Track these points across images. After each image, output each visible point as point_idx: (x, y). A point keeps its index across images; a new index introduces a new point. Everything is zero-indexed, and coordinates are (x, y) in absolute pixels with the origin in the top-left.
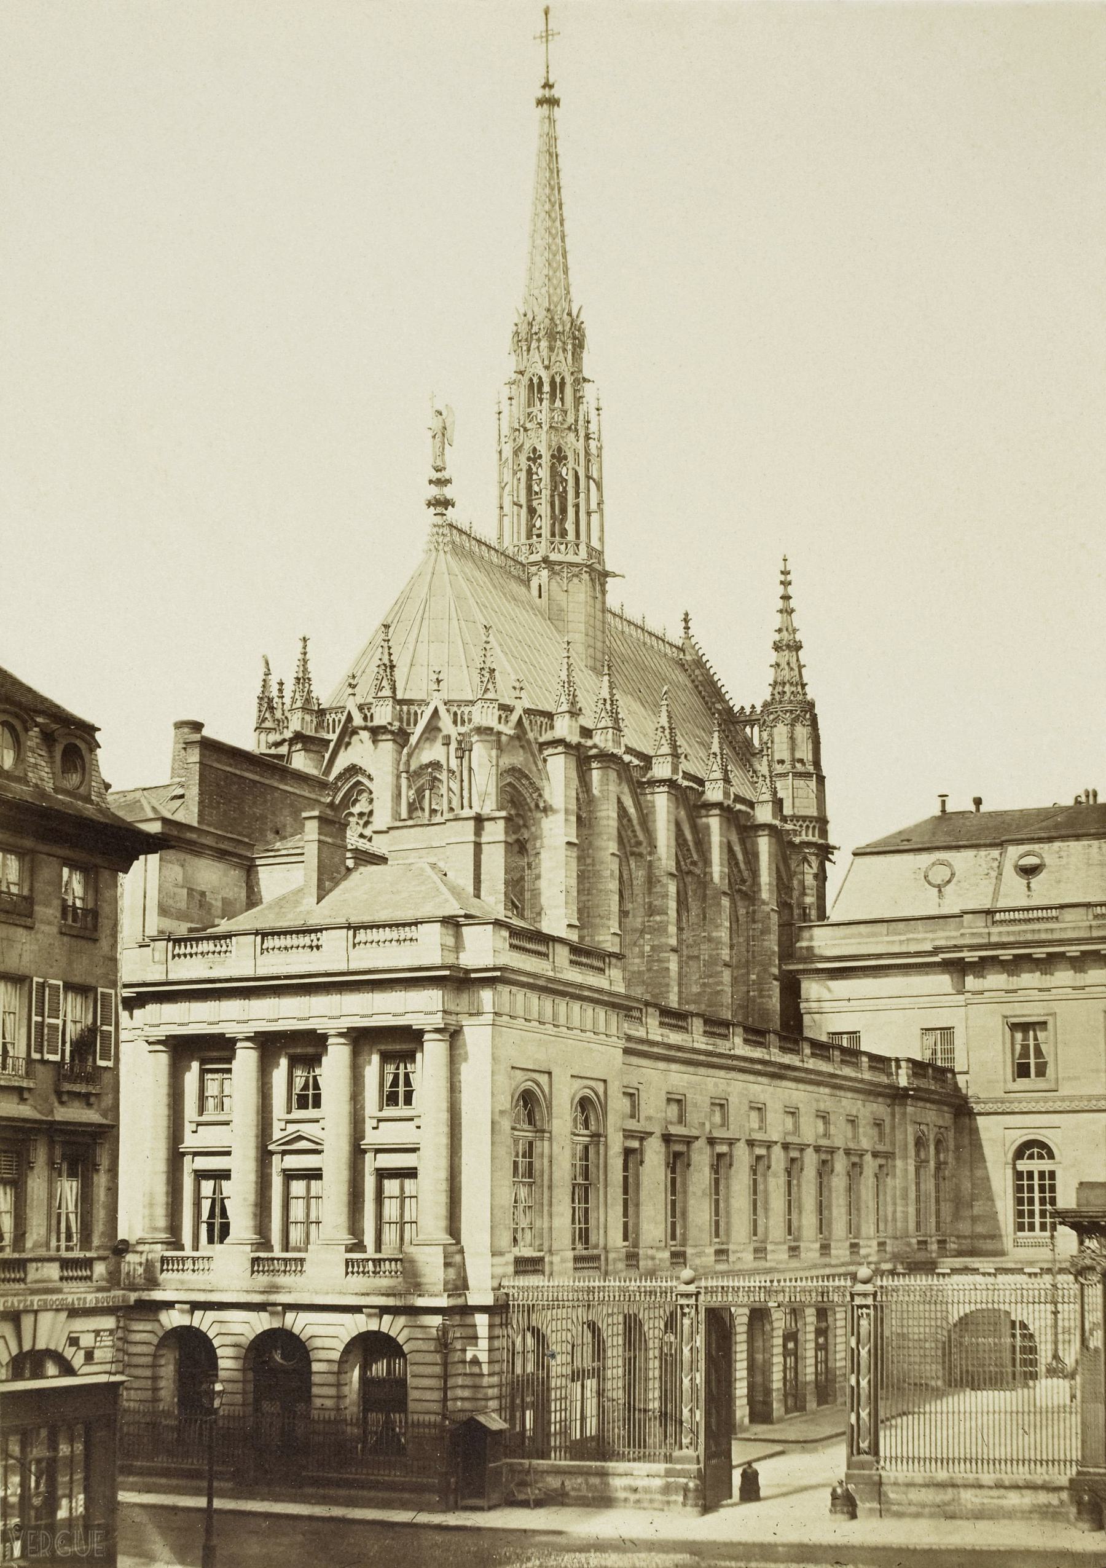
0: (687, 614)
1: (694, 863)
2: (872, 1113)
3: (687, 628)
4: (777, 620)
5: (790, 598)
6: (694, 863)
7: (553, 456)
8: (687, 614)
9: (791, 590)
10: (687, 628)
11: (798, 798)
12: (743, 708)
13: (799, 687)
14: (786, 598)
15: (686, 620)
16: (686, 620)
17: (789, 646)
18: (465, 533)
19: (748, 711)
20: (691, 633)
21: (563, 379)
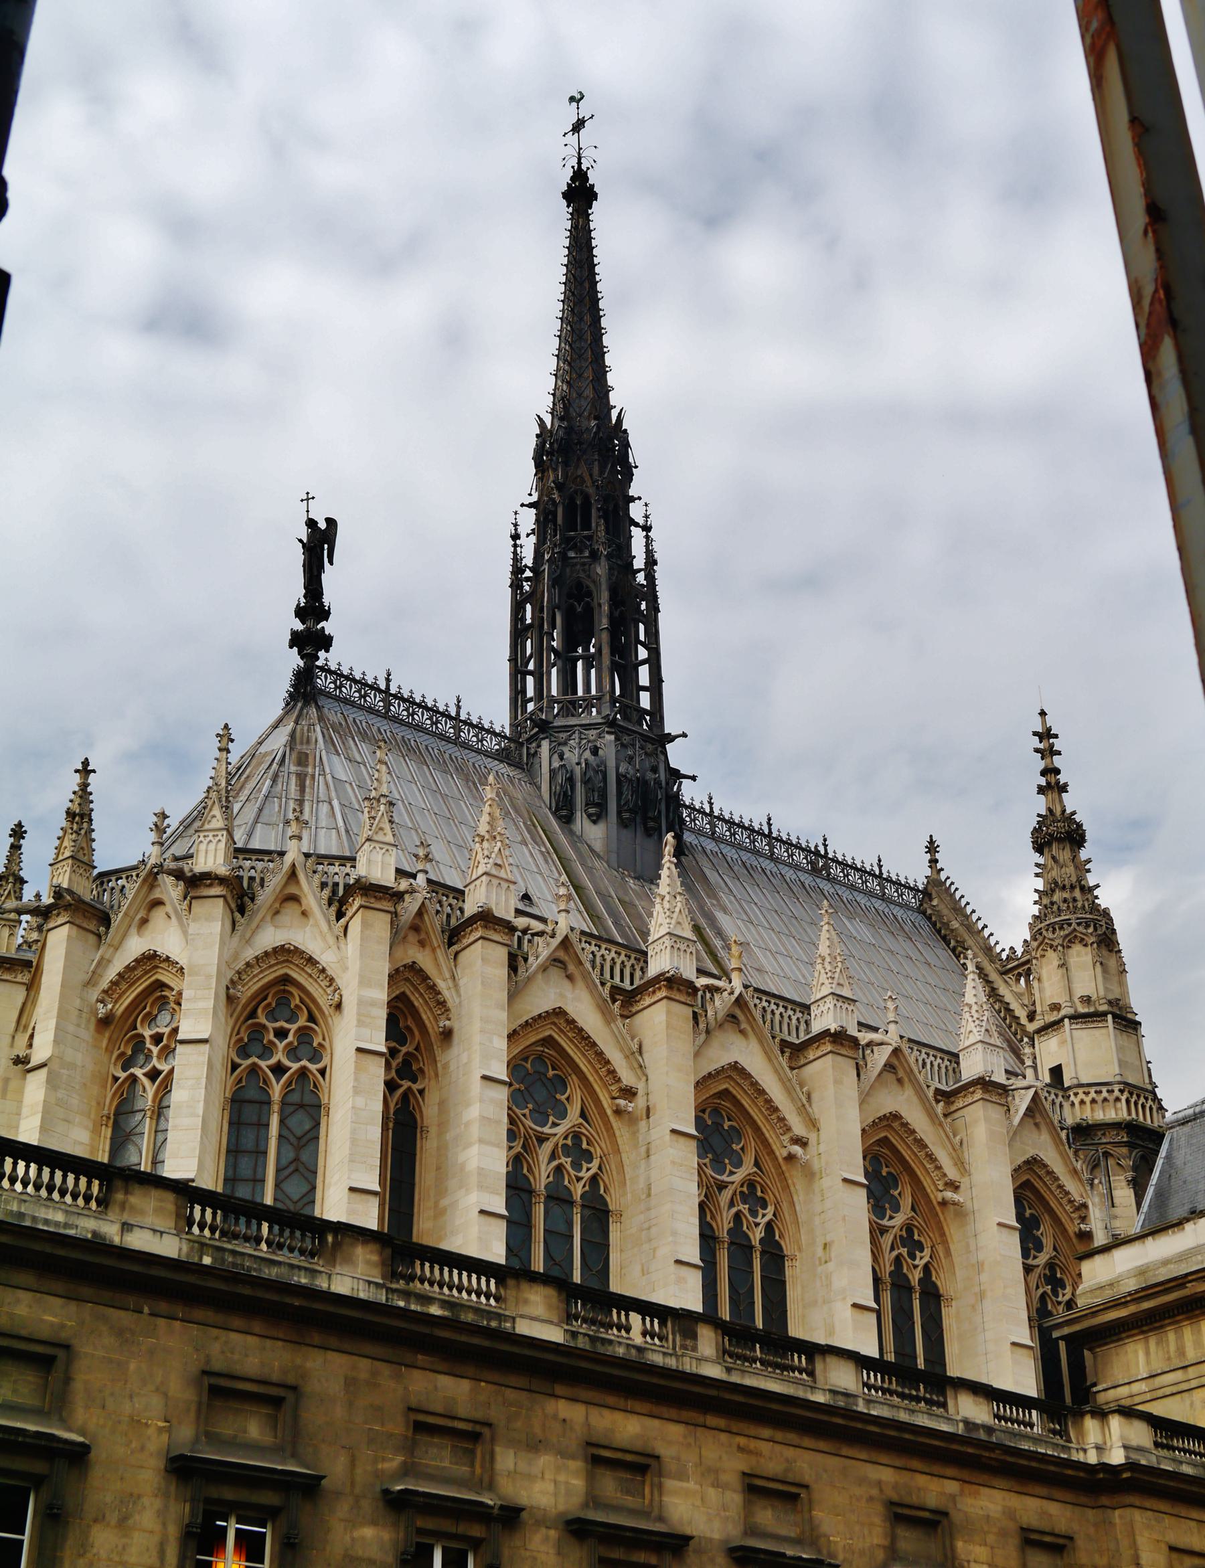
0: (931, 842)
1: (802, 1142)
2: (1010, 1514)
3: (934, 861)
4: (1040, 805)
5: (1057, 771)
6: (802, 1142)
7: (570, 596)
8: (931, 842)
9: (1057, 761)
10: (934, 861)
11: (1087, 1055)
12: (1012, 948)
13: (1077, 891)
14: (1050, 771)
15: (932, 848)
16: (932, 848)
17: (1059, 836)
18: (374, 687)
19: (1019, 951)
20: (939, 866)
21: (586, 498)
